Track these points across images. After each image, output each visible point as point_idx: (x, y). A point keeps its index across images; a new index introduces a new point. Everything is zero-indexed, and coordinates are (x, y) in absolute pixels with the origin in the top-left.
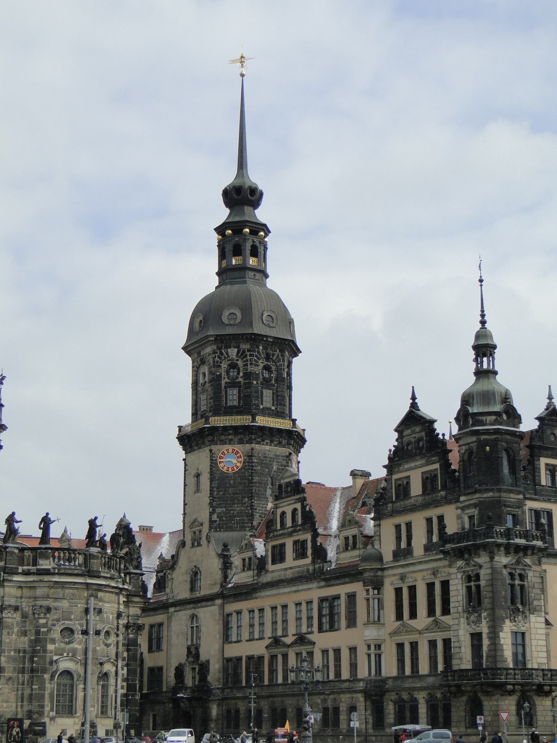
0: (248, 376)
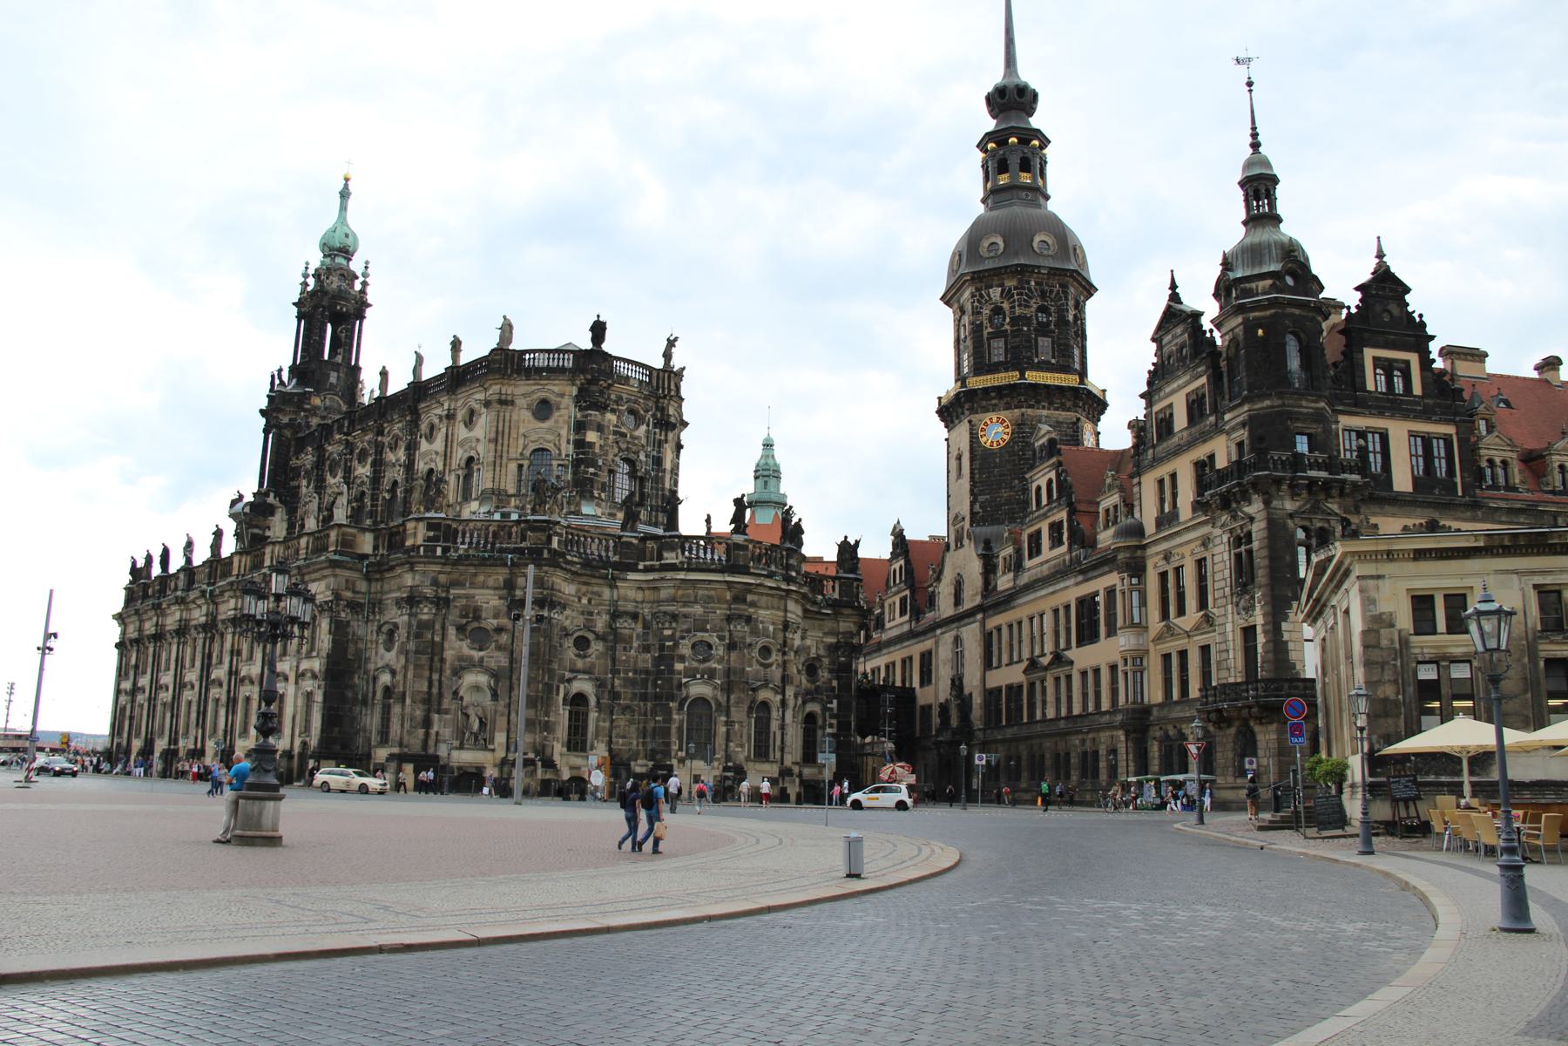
0: (1015, 320)
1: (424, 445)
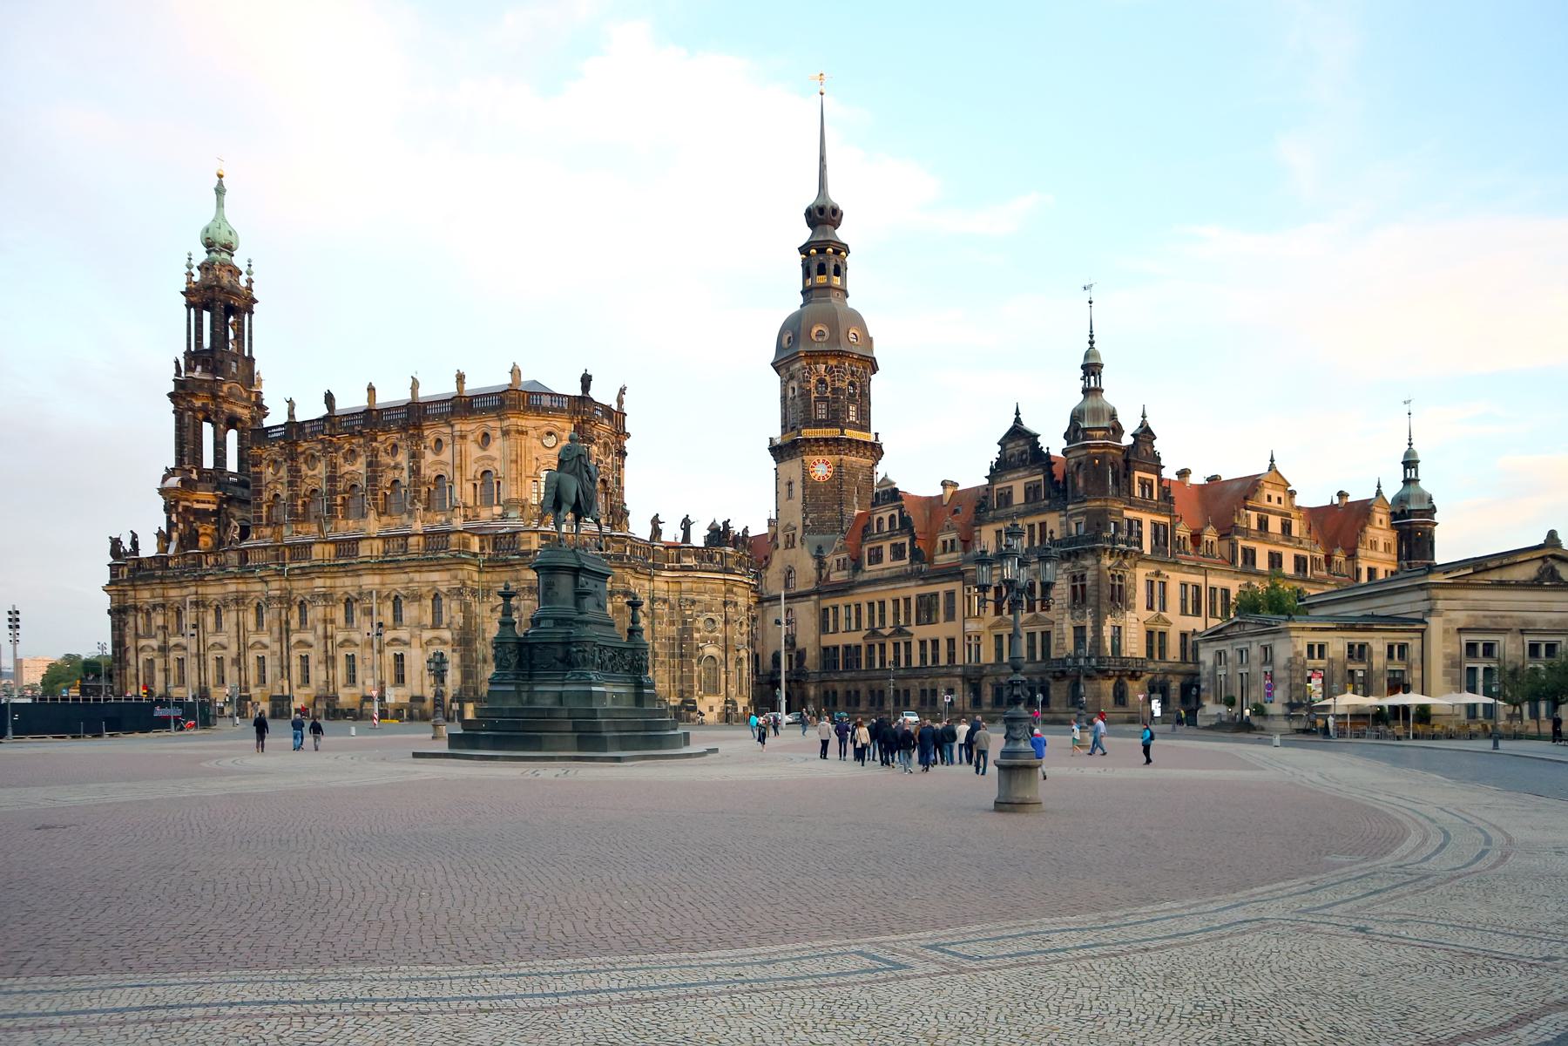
1: (429, 456)
